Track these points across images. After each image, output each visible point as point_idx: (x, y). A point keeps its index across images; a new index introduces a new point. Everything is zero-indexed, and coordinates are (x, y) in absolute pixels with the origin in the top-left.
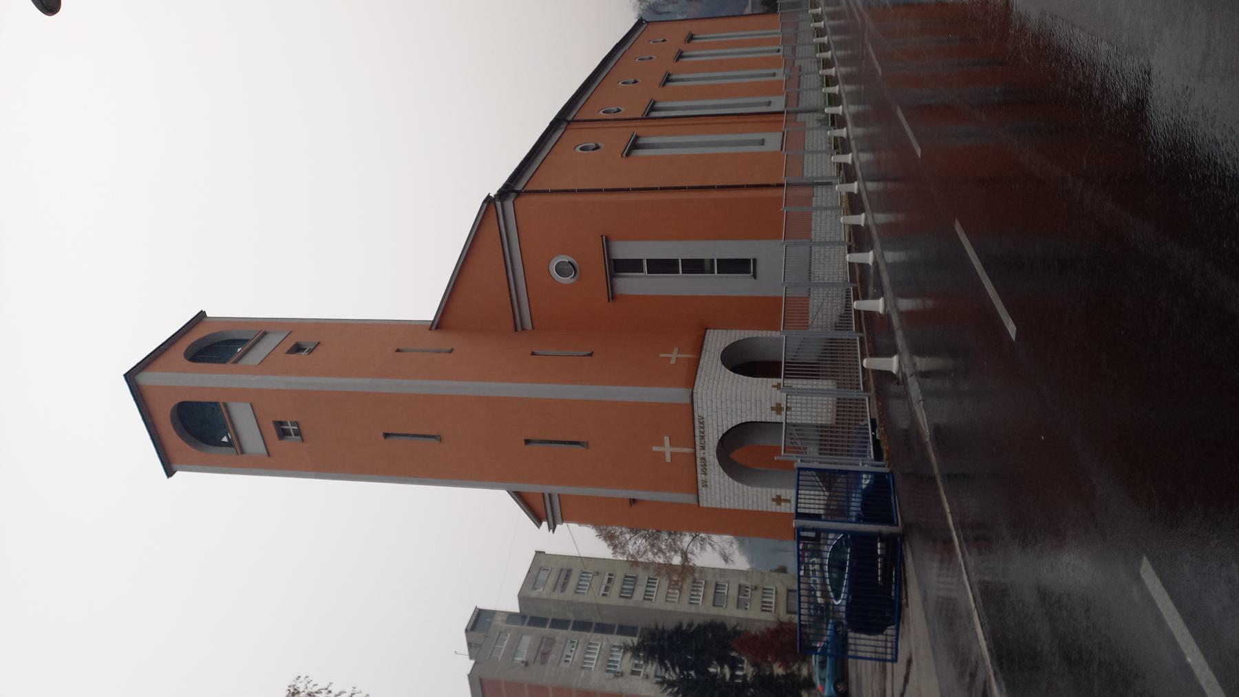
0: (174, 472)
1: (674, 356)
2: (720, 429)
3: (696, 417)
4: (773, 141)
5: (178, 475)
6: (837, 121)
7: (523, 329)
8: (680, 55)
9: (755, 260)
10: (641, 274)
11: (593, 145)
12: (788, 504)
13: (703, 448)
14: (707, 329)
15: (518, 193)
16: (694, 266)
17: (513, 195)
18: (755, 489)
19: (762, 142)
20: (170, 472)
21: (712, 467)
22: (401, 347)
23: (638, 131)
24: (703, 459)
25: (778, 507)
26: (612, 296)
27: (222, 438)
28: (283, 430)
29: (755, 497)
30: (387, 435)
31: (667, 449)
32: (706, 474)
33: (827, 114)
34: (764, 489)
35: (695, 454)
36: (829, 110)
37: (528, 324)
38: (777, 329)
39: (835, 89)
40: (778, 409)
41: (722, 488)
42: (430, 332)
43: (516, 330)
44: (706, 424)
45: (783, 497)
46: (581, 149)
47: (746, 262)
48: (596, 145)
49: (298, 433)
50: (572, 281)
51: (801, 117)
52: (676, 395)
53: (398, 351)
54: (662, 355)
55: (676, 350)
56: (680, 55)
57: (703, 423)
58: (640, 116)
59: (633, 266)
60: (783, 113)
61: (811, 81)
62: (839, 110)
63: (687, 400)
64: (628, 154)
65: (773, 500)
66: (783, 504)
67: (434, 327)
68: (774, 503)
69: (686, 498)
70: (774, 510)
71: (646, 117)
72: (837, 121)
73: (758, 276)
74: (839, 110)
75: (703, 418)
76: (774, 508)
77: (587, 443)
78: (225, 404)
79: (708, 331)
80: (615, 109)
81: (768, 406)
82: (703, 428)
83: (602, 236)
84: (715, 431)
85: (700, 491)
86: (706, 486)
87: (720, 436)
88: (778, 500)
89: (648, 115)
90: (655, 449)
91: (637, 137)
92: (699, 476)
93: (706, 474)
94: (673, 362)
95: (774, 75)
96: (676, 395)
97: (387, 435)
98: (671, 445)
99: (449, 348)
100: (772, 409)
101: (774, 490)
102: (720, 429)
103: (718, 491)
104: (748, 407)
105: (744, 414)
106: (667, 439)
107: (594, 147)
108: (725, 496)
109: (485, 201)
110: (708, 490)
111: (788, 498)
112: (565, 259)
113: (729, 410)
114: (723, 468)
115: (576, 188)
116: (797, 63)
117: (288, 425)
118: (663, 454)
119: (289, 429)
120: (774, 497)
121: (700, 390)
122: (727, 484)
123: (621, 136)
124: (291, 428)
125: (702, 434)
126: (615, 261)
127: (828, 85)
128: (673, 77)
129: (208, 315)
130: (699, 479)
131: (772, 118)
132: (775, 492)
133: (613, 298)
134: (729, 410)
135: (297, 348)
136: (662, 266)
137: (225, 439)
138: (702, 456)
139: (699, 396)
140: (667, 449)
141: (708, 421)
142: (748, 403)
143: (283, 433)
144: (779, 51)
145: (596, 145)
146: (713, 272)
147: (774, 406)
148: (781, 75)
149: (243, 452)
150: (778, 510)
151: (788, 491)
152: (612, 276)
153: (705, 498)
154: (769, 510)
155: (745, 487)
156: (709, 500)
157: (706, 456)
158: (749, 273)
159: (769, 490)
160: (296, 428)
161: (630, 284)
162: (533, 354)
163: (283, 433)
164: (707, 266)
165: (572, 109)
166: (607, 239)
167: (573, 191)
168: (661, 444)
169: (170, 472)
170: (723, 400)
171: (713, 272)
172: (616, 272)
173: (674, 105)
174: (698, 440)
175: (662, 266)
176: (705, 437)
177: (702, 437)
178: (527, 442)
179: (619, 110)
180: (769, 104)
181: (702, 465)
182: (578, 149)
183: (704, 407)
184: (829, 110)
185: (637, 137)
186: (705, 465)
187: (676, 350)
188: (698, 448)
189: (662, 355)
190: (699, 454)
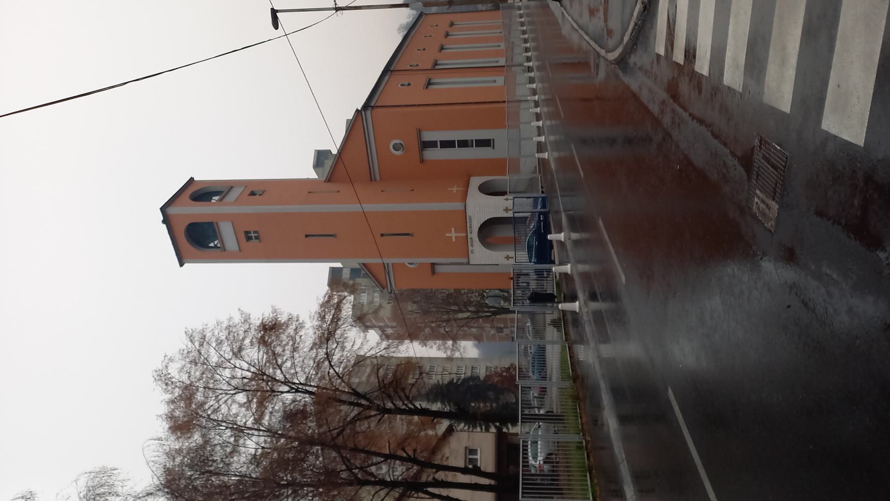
0: (184, 264)
1: (455, 189)
3: (467, 216)
4: (500, 81)
5: (186, 265)
6: (530, 69)
7: (375, 180)
8: (447, 35)
9: (493, 140)
10: (437, 149)
11: (407, 83)
13: (471, 233)
14: (470, 177)
16: (464, 144)
19: (495, 81)
20: (181, 265)
22: (311, 191)
23: (430, 76)
25: (508, 261)
26: (422, 161)
27: (210, 243)
28: (249, 236)
30: (307, 236)
31: (453, 235)
33: (525, 66)
34: (501, 252)
36: (526, 64)
37: (378, 178)
38: (505, 175)
39: (529, 54)
40: (507, 210)
42: (325, 184)
43: (371, 181)
44: (472, 220)
45: (510, 256)
46: (401, 85)
47: (490, 140)
48: (409, 83)
49: (257, 238)
50: (402, 153)
51: (514, 69)
52: (457, 206)
53: (309, 192)
54: (449, 189)
55: (456, 187)
56: (447, 35)
57: (471, 219)
58: (430, 68)
59: (432, 144)
60: (504, 66)
61: (518, 50)
62: (531, 64)
63: (464, 209)
64: (427, 88)
65: (505, 258)
66: (510, 259)
67: (327, 181)
68: (506, 259)
69: (464, 260)
71: (433, 69)
72: (530, 69)
74: (531, 64)
76: (505, 262)
78: (217, 223)
79: (471, 178)
80: (415, 64)
82: (471, 222)
83: (417, 129)
86: (472, 253)
88: (508, 258)
89: (434, 67)
90: (447, 235)
91: (430, 79)
92: (469, 247)
94: (455, 191)
95: (499, 46)
96: (457, 206)
97: (307, 236)
98: (456, 232)
99: (337, 190)
100: (504, 210)
101: (505, 252)
106: (453, 229)
107: (408, 84)
111: (512, 256)
112: (398, 141)
114: (481, 243)
116: (511, 40)
117: (251, 233)
118: (451, 237)
119: (252, 236)
123: (422, 79)
124: (253, 235)
126: (424, 142)
127: (526, 52)
128: (444, 47)
129: (195, 179)
131: (499, 69)
132: (506, 253)
135: (253, 194)
136: (447, 144)
137: (212, 245)
140: (453, 235)
143: (249, 238)
144: (501, 33)
145: (409, 83)
147: (505, 208)
148: (503, 46)
149: (225, 250)
152: (422, 150)
155: (492, 252)
157: (473, 237)
158: (490, 146)
159: (503, 252)
160: (256, 235)
161: (432, 154)
162: (382, 191)
163: (249, 238)
164: (470, 143)
165: (393, 63)
166: (419, 131)
168: (451, 232)
169: (181, 265)
171: (473, 147)
173: (447, 62)
174: (468, 228)
175: (447, 144)
177: (471, 227)
179: (418, 65)
180: (497, 62)
182: (399, 85)
184: (526, 64)
185: (430, 79)
187: (456, 187)
188: (468, 232)
189: (449, 189)
190: (469, 237)
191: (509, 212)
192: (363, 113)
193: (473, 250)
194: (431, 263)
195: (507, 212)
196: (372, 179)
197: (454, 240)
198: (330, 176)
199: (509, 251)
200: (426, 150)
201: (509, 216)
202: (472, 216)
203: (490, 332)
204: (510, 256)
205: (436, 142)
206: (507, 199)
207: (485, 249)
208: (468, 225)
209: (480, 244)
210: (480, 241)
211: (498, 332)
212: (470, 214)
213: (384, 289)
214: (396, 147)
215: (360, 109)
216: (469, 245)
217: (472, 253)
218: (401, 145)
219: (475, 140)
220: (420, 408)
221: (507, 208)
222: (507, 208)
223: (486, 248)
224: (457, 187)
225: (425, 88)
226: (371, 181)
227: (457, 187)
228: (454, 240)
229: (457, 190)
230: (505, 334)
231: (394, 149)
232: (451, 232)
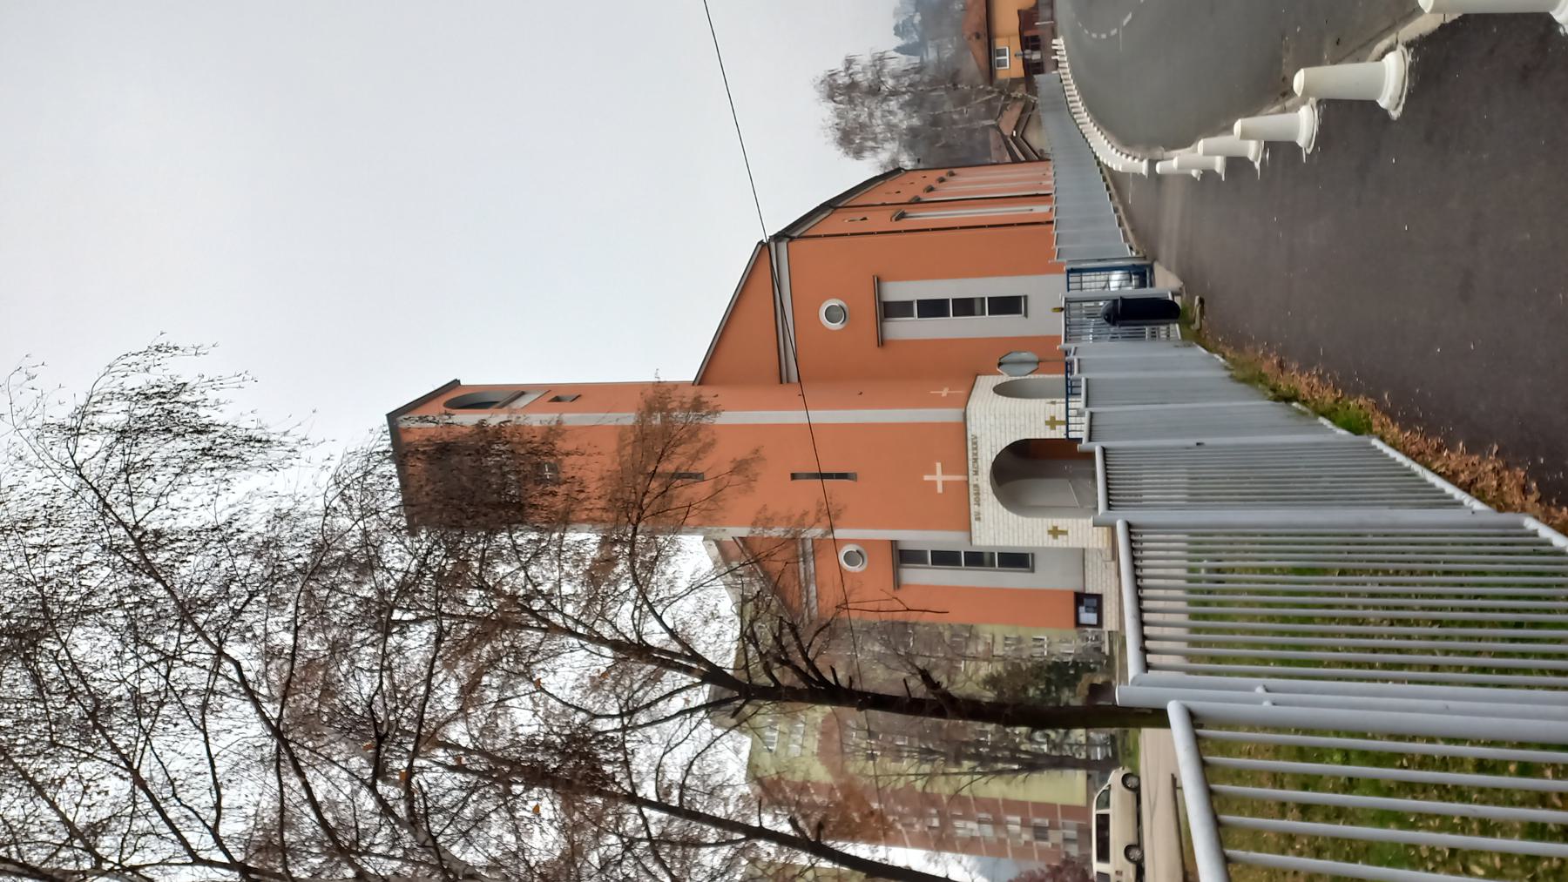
1: (944, 393)
2: (994, 449)
3: (969, 436)
9: (1026, 297)
12: (1065, 537)
13: (976, 473)
14: (978, 375)
15: (792, 239)
16: (965, 307)
17: (788, 239)
24: (976, 486)
26: (882, 342)
29: (1030, 530)
31: (939, 478)
32: (979, 505)
34: (1040, 520)
35: (967, 482)
40: (1052, 423)
41: (996, 520)
44: (979, 444)
45: (1059, 529)
52: (950, 415)
57: (975, 443)
59: (903, 309)
63: (960, 419)
65: (1050, 532)
68: (1051, 536)
70: (1050, 545)
73: (1029, 315)
77: (856, 475)
81: (1043, 421)
82: (976, 449)
87: (994, 457)
90: (927, 478)
93: (979, 505)
96: (950, 415)
98: (944, 472)
100: (1047, 423)
101: (1050, 520)
102: (994, 449)
103: (992, 525)
104: (1023, 422)
105: (1018, 431)
106: (939, 465)
109: (759, 243)
110: (982, 524)
111: (1065, 529)
112: (835, 302)
113: (1003, 428)
115: (849, 232)
118: (934, 483)
120: (1051, 529)
121: (973, 408)
122: (1001, 517)
126: (886, 304)
130: (972, 511)
134: (1003, 428)
136: (932, 308)
139: (972, 411)
142: (1023, 418)
146: (983, 314)
147: (1048, 419)
150: (1055, 545)
151: (1065, 520)
153: (978, 534)
154: (1045, 545)
155: (1020, 518)
156: (983, 537)
157: (979, 483)
158: (1020, 312)
159: (1045, 520)
161: (904, 329)
164: (977, 307)
167: (846, 235)
168: (933, 472)
170: (997, 416)
171: (983, 314)
172: (886, 316)
174: (970, 463)
175: (932, 308)
177: (975, 460)
178: (794, 476)
181: (975, 494)
183: (978, 425)
186: (978, 494)
188: (971, 473)
191: (1057, 427)
193: (979, 514)
194: (892, 541)
195: (1053, 428)
196: (782, 378)
197: (940, 489)
201: (1058, 437)
203: (1019, 836)
204: (1059, 529)
205: (910, 303)
206: (1054, 403)
207: (1005, 510)
210: (995, 493)
211: (1037, 838)
214: (830, 314)
216: (972, 498)
219: (989, 298)
220: (834, 683)
221: (1053, 418)
222: (1053, 418)
223: (1006, 507)
228: (940, 489)
230: (1053, 845)
232: (933, 472)
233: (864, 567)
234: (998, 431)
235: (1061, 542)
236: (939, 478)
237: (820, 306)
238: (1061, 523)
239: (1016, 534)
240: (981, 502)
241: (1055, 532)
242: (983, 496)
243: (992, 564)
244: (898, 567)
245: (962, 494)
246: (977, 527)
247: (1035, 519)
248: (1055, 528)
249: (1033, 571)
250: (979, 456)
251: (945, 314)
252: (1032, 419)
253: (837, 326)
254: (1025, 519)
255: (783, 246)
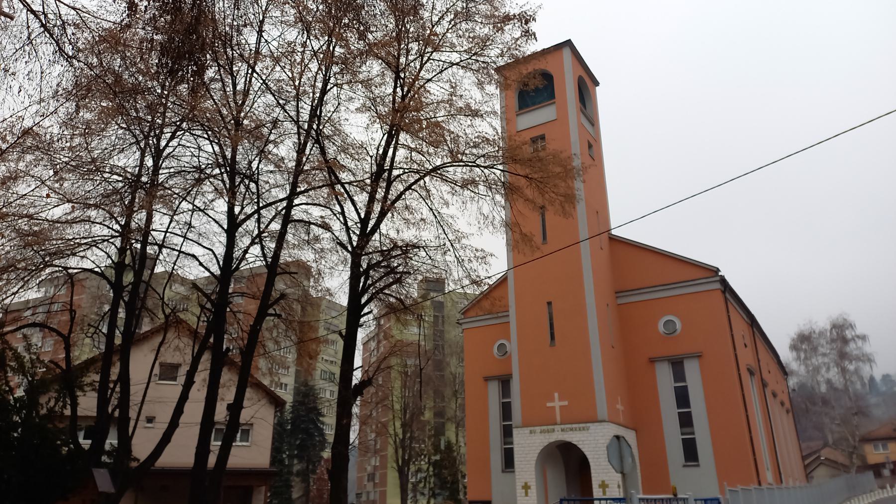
1: (620, 407)
2: (581, 443)
3: (588, 425)
7: (617, 297)
13: (563, 430)
14: (636, 431)
17: (723, 289)
18: (534, 469)
21: (548, 437)
24: (554, 430)
26: (652, 361)
32: (541, 432)
34: (534, 476)
35: (556, 424)
41: (531, 445)
43: (616, 293)
45: (529, 490)
57: (584, 429)
59: (679, 374)
63: (600, 418)
65: (526, 483)
66: (524, 490)
68: (523, 484)
70: (518, 484)
75: (588, 430)
77: (554, 346)
82: (580, 430)
83: (701, 352)
84: (578, 439)
85: (526, 428)
86: (531, 432)
88: (526, 487)
90: (556, 395)
93: (541, 432)
96: (602, 409)
98: (561, 407)
101: (534, 484)
102: (581, 443)
103: (528, 442)
106: (566, 403)
108: (524, 447)
109: (718, 269)
110: (528, 435)
111: (529, 494)
112: (679, 326)
120: (529, 484)
125: (574, 429)
133: (652, 361)
136: (682, 397)
138: (556, 430)
140: (557, 403)
141: (585, 433)
150: (518, 487)
151: (535, 494)
153: (521, 432)
154: (517, 480)
155: (534, 462)
156: (520, 435)
157: (556, 433)
159: (534, 480)
161: (664, 375)
162: (608, 305)
168: (561, 399)
175: (682, 397)
176: (571, 432)
177: (571, 430)
186: (548, 431)
188: (563, 426)
189: (619, 398)
190: (557, 427)
192: (718, 278)
193: (535, 433)
198: (615, 239)
199: (537, 488)
200: (669, 367)
202: (590, 431)
204: (529, 490)
205: (684, 380)
208: (574, 426)
209: (546, 444)
210: (550, 444)
212: (591, 428)
213: (462, 314)
215: (720, 274)
217: (531, 432)
218: (675, 332)
224: (622, 411)
225: (748, 367)
226: (616, 293)
227: (622, 411)
228: (549, 405)
229: (618, 409)
231: (671, 320)
232: (561, 399)
233: (496, 356)
234: (594, 445)
235: (520, 492)
236: (557, 403)
237: (678, 317)
238: (533, 492)
239: (523, 459)
240: (543, 434)
241: (526, 487)
242: (547, 435)
243: (505, 444)
244: (499, 379)
245: (547, 421)
246: (526, 432)
247: (534, 473)
248: (529, 488)
249: (503, 471)
250: (575, 432)
251: (679, 406)
252: (605, 471)
253: (661, 328)
254: (534, 466)
255: (718, 286)
